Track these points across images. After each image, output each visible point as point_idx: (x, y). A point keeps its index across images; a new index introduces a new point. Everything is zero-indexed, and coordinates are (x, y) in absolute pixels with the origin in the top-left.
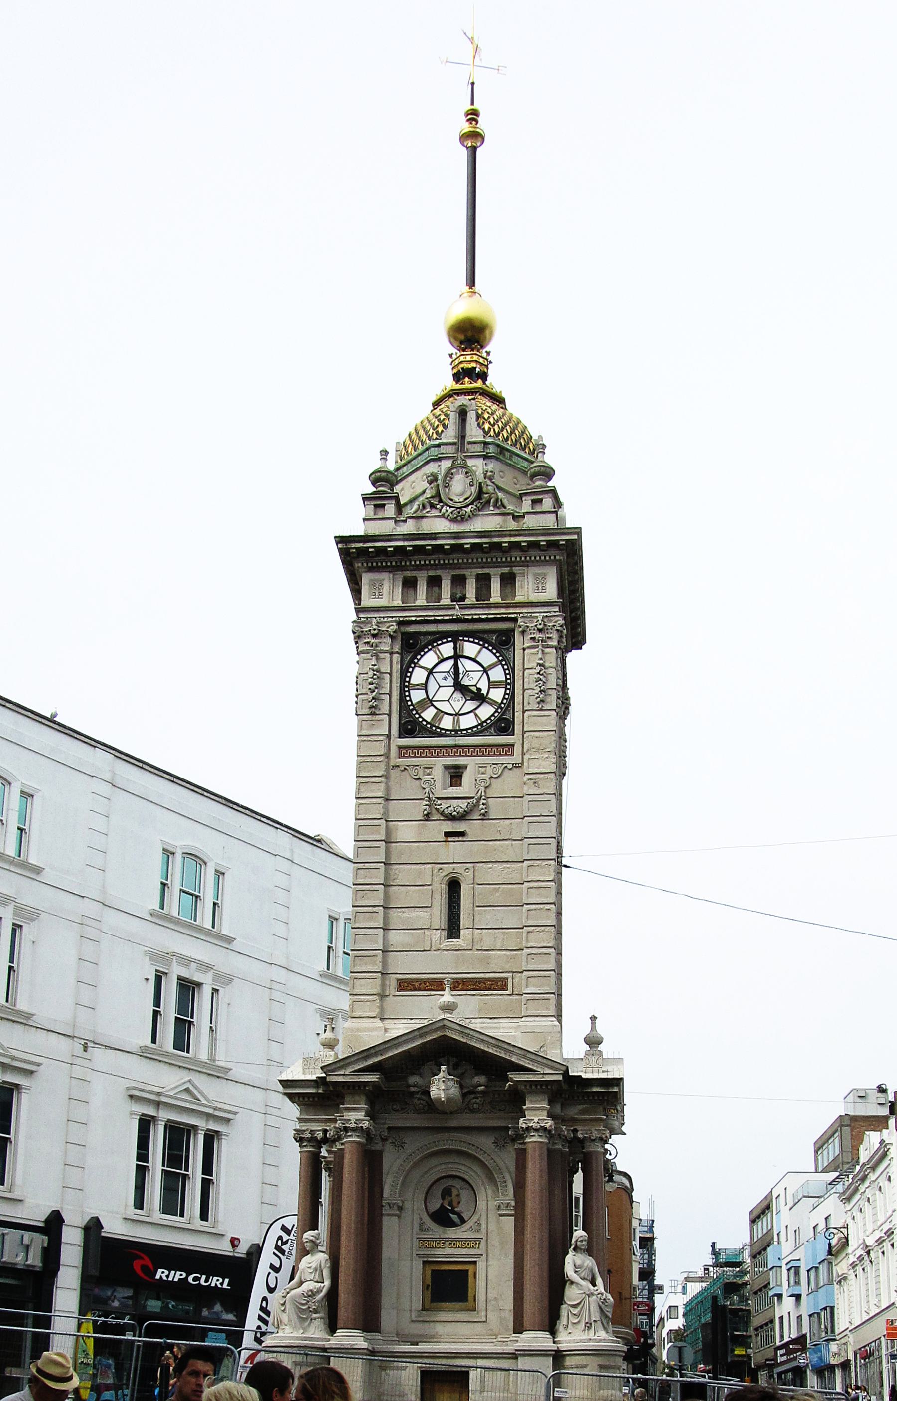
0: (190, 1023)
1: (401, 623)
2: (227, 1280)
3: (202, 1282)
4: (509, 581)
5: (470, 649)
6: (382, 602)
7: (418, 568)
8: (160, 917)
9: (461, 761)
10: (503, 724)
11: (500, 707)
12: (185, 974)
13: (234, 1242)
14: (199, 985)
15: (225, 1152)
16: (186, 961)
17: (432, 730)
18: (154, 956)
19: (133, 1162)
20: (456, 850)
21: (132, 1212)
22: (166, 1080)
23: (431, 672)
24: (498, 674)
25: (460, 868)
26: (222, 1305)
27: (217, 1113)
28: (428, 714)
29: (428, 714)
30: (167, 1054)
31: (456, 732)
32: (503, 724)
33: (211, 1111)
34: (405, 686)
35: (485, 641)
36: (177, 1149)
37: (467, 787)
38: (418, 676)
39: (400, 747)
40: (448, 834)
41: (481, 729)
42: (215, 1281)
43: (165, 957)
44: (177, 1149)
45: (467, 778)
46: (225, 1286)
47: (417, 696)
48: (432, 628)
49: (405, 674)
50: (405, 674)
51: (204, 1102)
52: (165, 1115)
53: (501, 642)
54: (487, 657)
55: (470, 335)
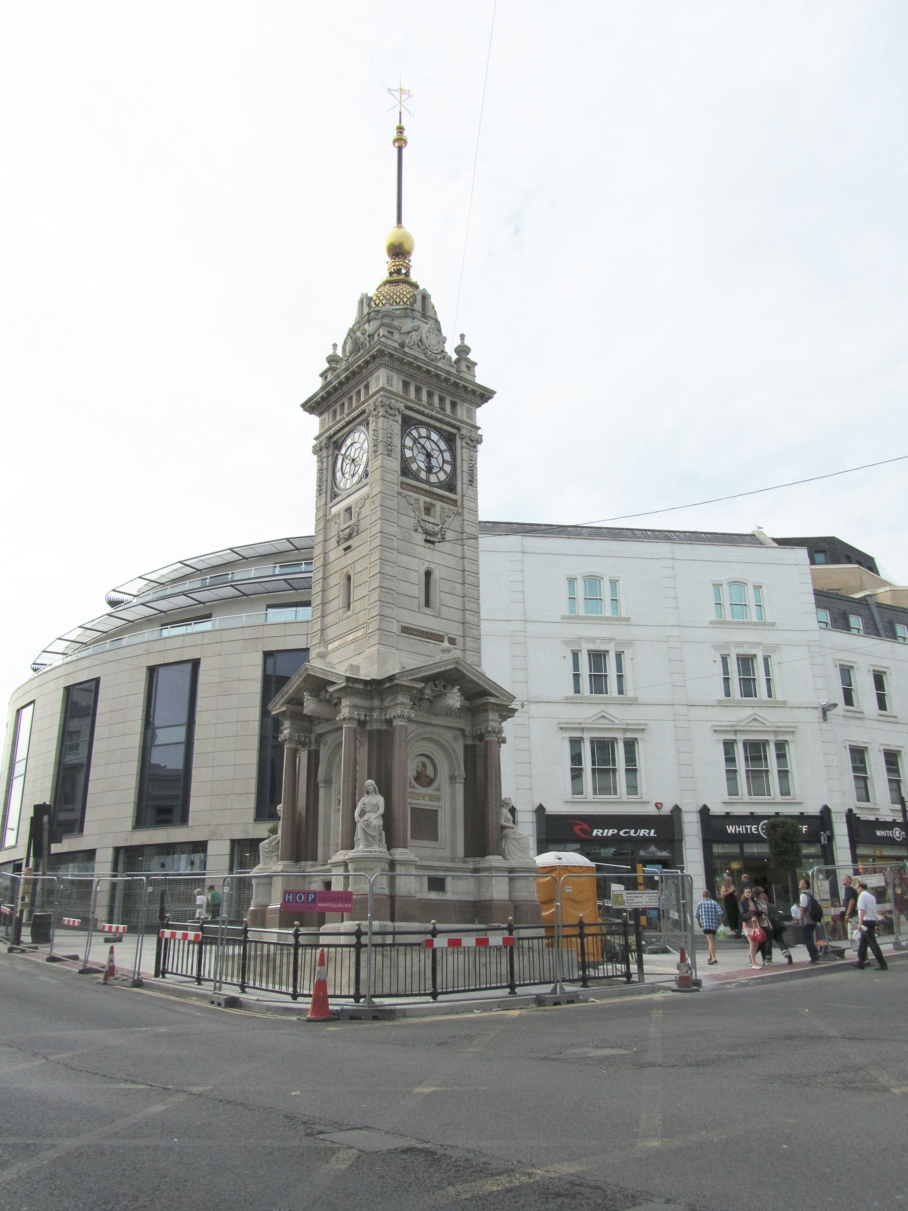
0: (754, 679)
2: (653, 831)
3: (632, 833)
4: (367, 387)
7: (336, 402)
8: (719, 623)
12: (741, 651)
13: (658, 806)
14: (755, 656)
15: (791, 751)
16: (741, 644)
18: (716, 647)
19: (722, 766)
20: (351, 556)
21: (727, 798)
22: (740, 715)
26: (656, 847)
27: (780, 729)
30: (766, 702)
33: (776, 729)
36: (756, 755)
40: (345, 549)
42: (642, 832)
43: (727, 645)
44: (756, 755)
46: (652, 834)
48: (341, 433)
51: (768, 724)
52: (740, 738)
55: (399, 251)
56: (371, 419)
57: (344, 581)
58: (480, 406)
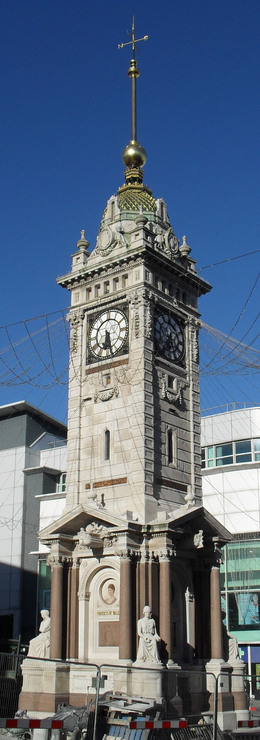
1: (85, 310)
5: (113, 315)
11: (124, 340)
17: (99, 359)
23: (98, 330)
24: (123, 324)
28: (97, 352)
32: (125, 349)
34: (89, 339)
35: (119, 309)
38: (94, 333)
39: (87, 371)
47: (93, 343)
49: (89, 334)
50: (89, 334)
53: (124, 309)
54: (119, 317)
56: (131, 306)
57: (104, 435)
58: (199, 296)
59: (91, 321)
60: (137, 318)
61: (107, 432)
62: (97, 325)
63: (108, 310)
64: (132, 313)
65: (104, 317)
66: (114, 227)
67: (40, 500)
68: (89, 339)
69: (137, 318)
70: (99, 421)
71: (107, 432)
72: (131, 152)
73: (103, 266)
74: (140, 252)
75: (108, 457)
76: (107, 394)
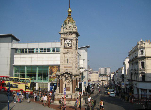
5: (69, 40)
6: (62, 37)
9: (68, 50)
10: (71, 46)
25: (68, 58)
29: (66, 46)
31: (68, 47)
32: (71, 46)
34: (64, 43)
37: (69, 52)
38: (65, 43)
41: (70, 47)
45: (69, 51)
47: (65, 44)
49: (64, 42)
50: (64, 42)
53: (71, 40)
54: (70, 41)
56: (73, 40)
59: (65, 40)
60: (74, 43)
61: (68, 59)
62: (66, 41)
63: (68, 39)
64: (73, 41)
65: (67, 40)
66: (69, 25)
67: (14, 54)
68: (64, 43)
69: (74, 43)
70: (66, 57)
71: (68, 59)
72: (70, 10)
73: (68, 32)
74: (75, 32)
75: (68, 63)
76: (68, 53)
